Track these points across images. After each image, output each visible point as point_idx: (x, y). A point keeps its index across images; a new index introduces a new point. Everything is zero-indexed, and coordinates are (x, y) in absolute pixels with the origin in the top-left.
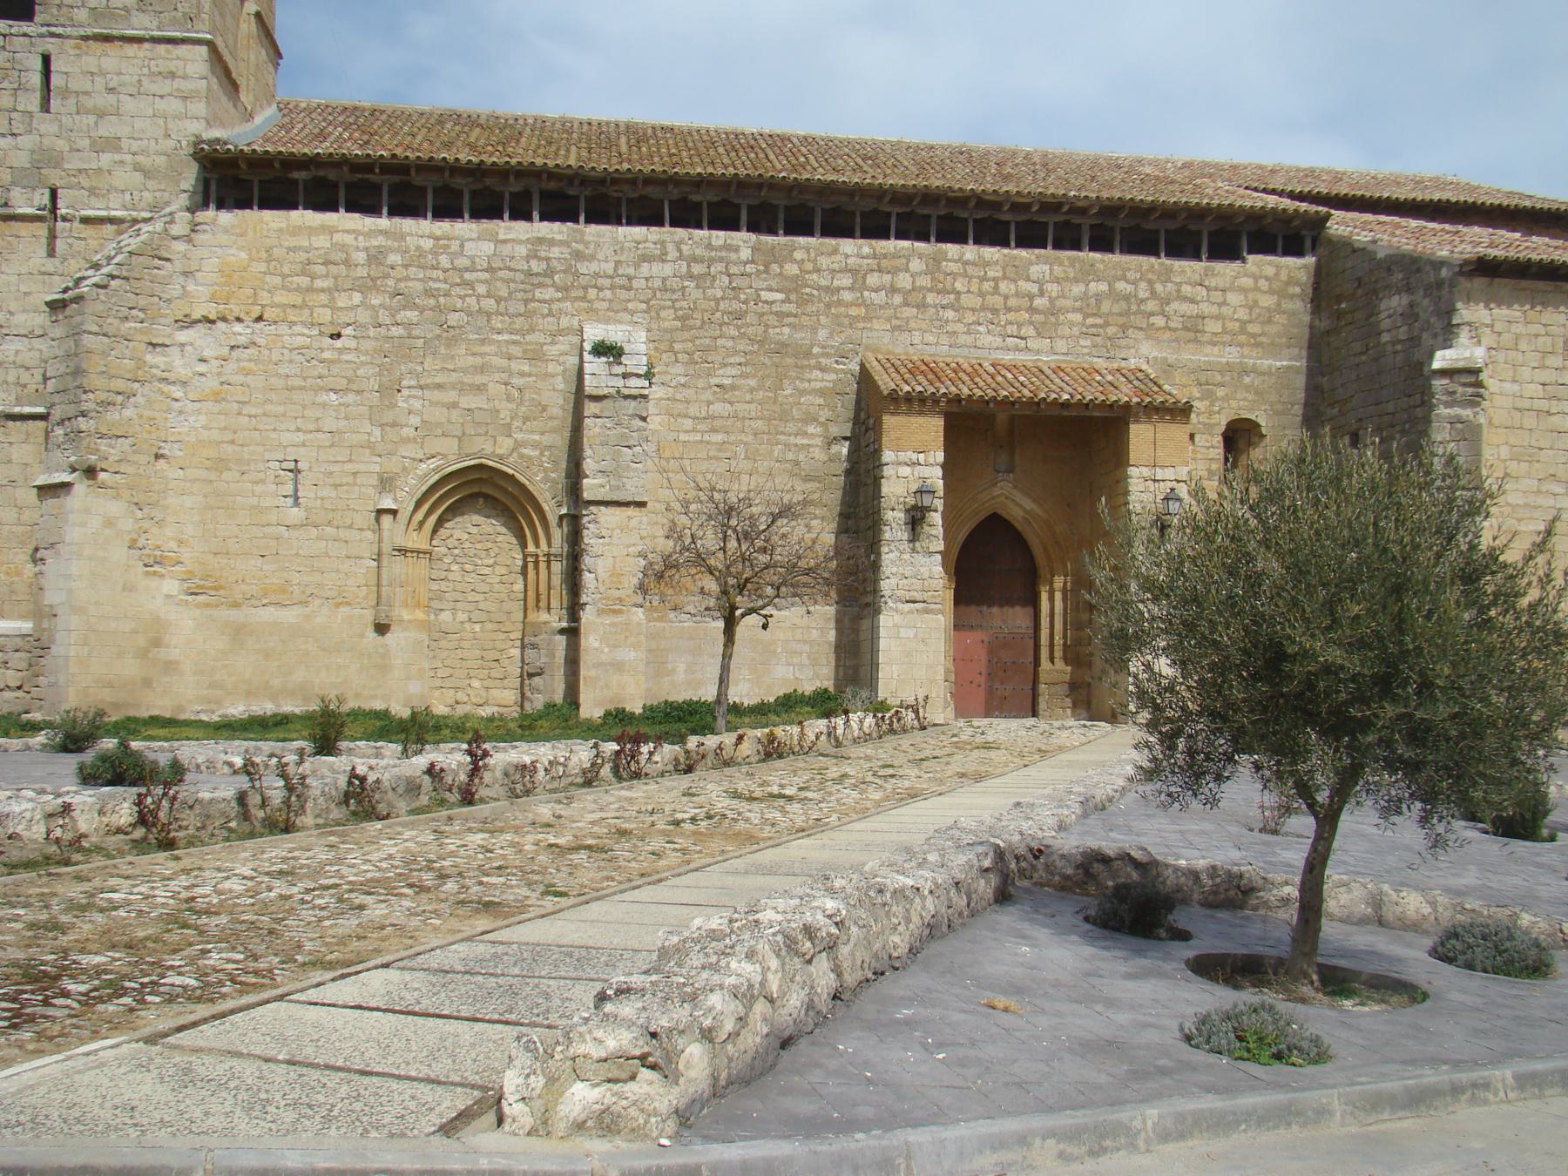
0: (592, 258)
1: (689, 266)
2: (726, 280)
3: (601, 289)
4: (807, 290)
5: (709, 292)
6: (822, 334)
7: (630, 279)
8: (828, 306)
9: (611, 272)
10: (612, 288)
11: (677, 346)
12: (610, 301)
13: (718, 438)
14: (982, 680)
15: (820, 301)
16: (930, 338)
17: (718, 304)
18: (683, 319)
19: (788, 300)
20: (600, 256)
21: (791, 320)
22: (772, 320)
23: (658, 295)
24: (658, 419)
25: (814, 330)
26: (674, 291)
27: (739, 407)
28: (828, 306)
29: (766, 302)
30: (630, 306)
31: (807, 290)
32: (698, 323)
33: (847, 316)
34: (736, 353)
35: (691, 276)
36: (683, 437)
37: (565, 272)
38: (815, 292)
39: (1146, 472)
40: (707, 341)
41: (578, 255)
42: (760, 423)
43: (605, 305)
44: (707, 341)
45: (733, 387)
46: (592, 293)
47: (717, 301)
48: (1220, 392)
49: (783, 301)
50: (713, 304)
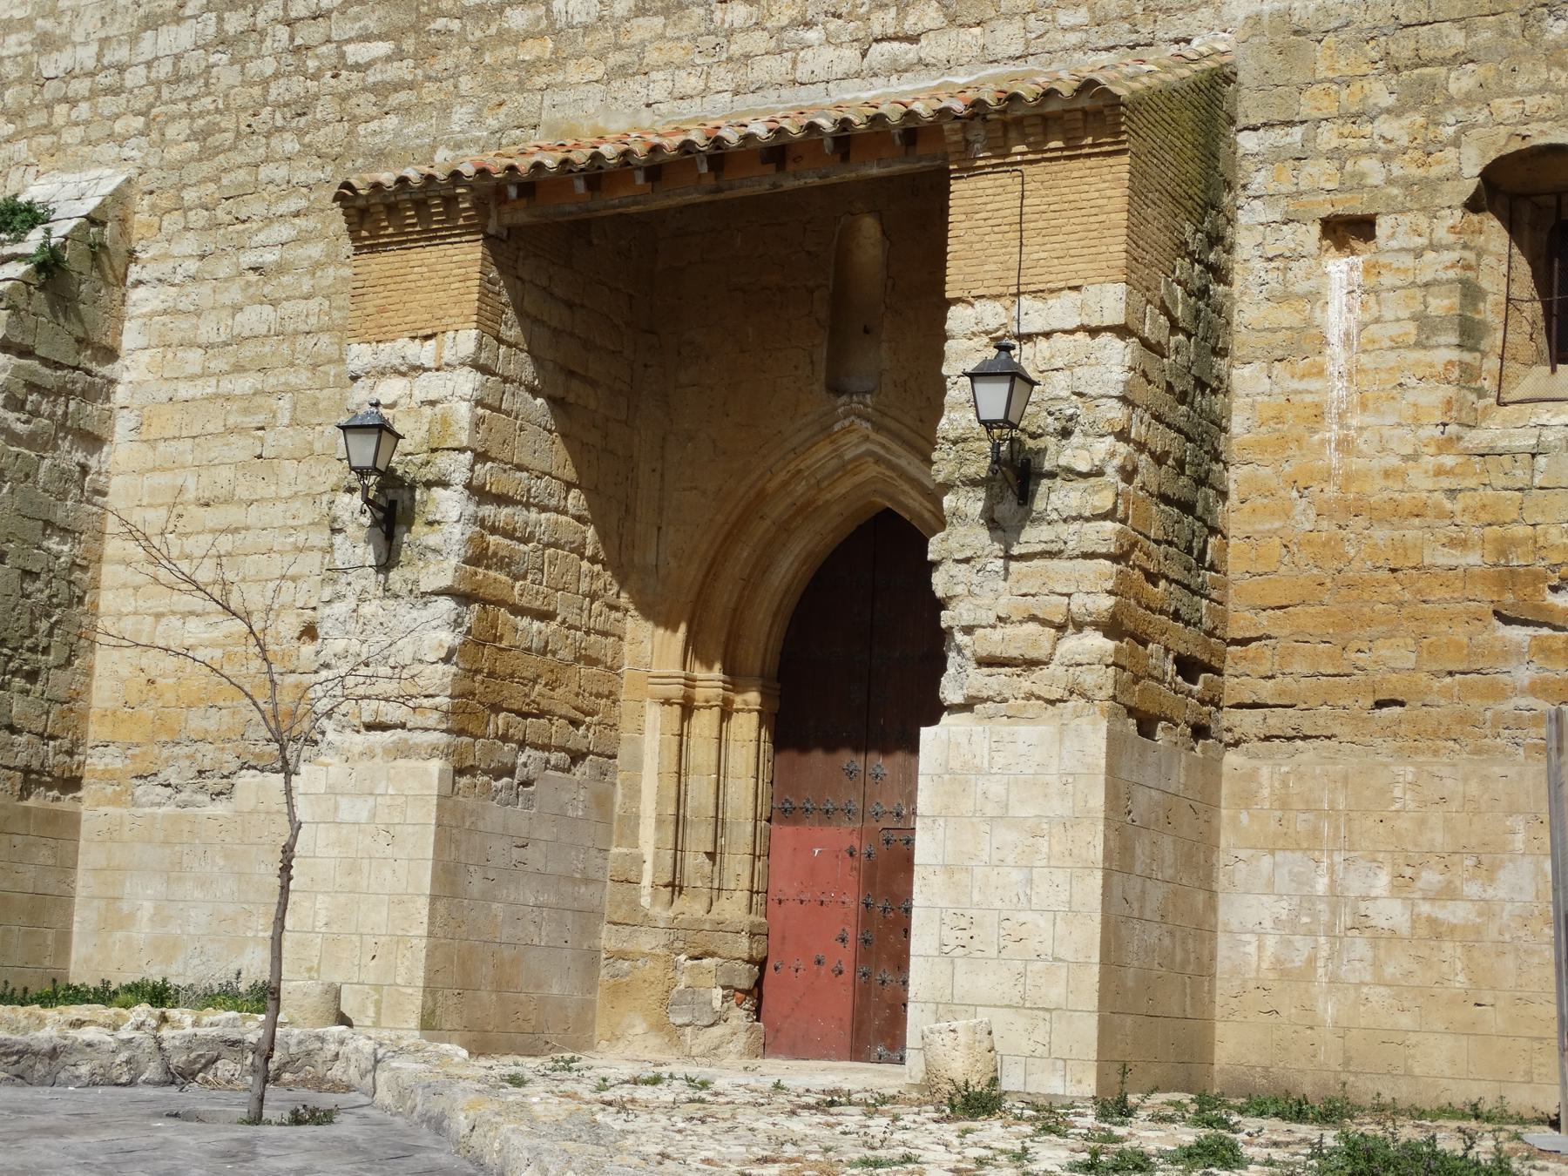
0: (66, 40)
1: (220, 19)
2: (283, 32)
3: (73, 102)
4: (440, 23)
5: (253, 67)
6: (461, 115)
7: (121, 69)
8: (478, 50)
9: (90, 64)
10: (93, 94)
11: (190, 196)
12: (87, 123)
13: (244, 384)
14: (846, 956)
15: (463, 41)
16: (691, 83)
17: (266, 91)
18: (201, 136)
19: (399, 55)
20: (78, 37)
21: (402, 97)
22: (364, 104)
23: (165, 93)
24: (144, 357)
25: (446, 110)
26: (190, 78)
27: (288, 308)
28: (478, 50)
29: (357, 67)
30: (119, 127)
31: (440, 23)
32: (230, 136)
33: (518, 64)
34: (291, 186)
35: (223, 41)
36: (184, 390)
37: (20, 80)
38: (455, 25)
39: (992, 315)
40: (241, 175)
41: (46, 43)
42: (325, 338)
43: (78, 132)
44: (241, 175)
45: (281, 268)
46: (61, 110)
47: (265, 83)
48: (1461, 82)
49: (388, 59)
50: (257, 91)
